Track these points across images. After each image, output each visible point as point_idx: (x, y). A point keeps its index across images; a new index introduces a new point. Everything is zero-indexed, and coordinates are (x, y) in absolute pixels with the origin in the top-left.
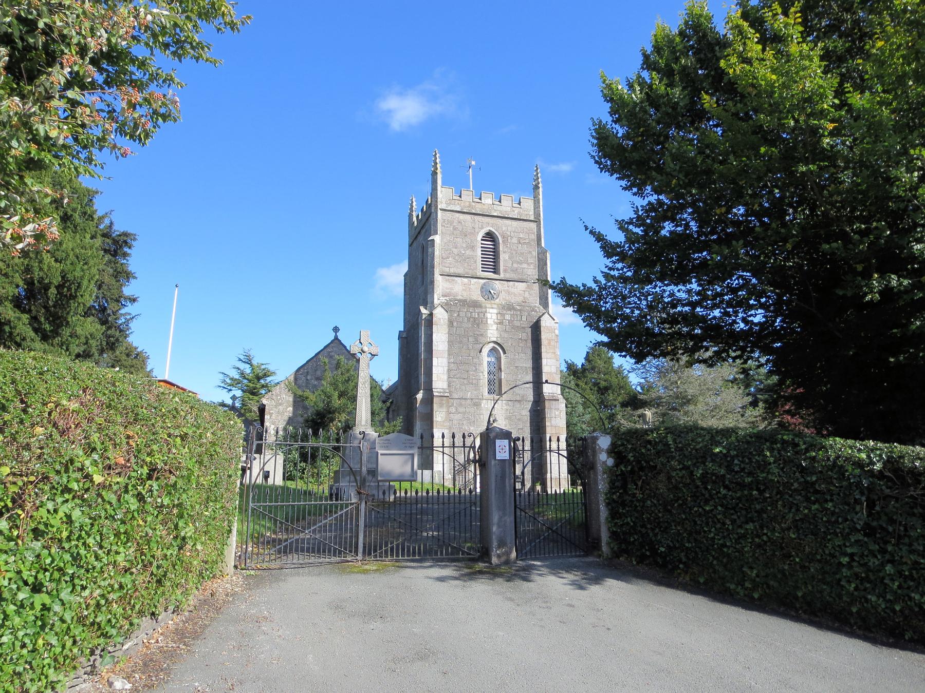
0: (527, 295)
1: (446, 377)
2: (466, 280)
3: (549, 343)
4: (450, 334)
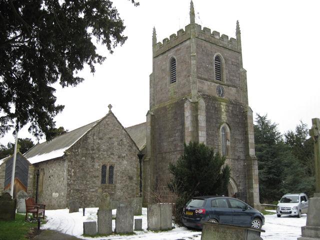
2: (209, 83)
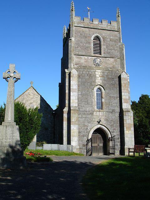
0: (114, 63)
1: (77, 101)
2: (86, 57)
3: (125, 86)
4: (78, 82)
